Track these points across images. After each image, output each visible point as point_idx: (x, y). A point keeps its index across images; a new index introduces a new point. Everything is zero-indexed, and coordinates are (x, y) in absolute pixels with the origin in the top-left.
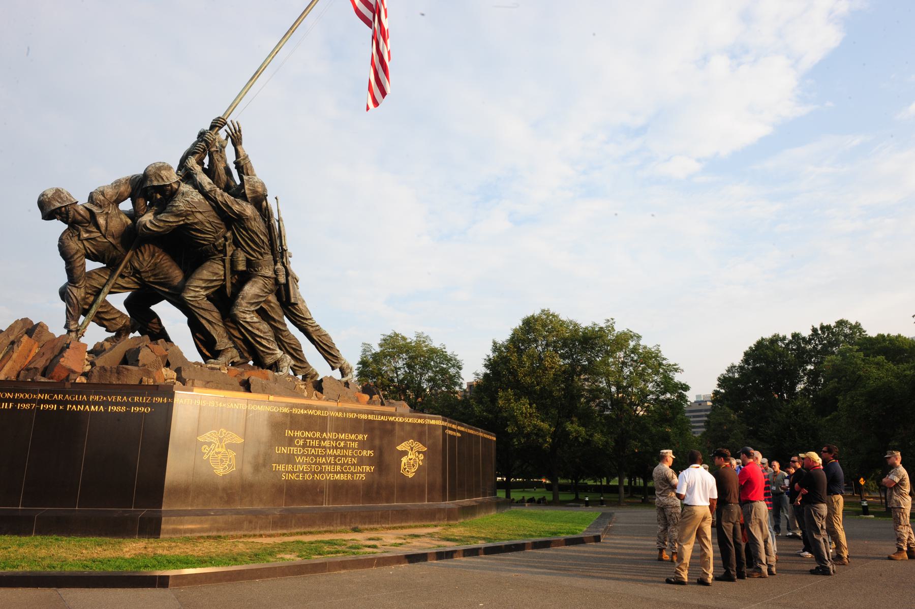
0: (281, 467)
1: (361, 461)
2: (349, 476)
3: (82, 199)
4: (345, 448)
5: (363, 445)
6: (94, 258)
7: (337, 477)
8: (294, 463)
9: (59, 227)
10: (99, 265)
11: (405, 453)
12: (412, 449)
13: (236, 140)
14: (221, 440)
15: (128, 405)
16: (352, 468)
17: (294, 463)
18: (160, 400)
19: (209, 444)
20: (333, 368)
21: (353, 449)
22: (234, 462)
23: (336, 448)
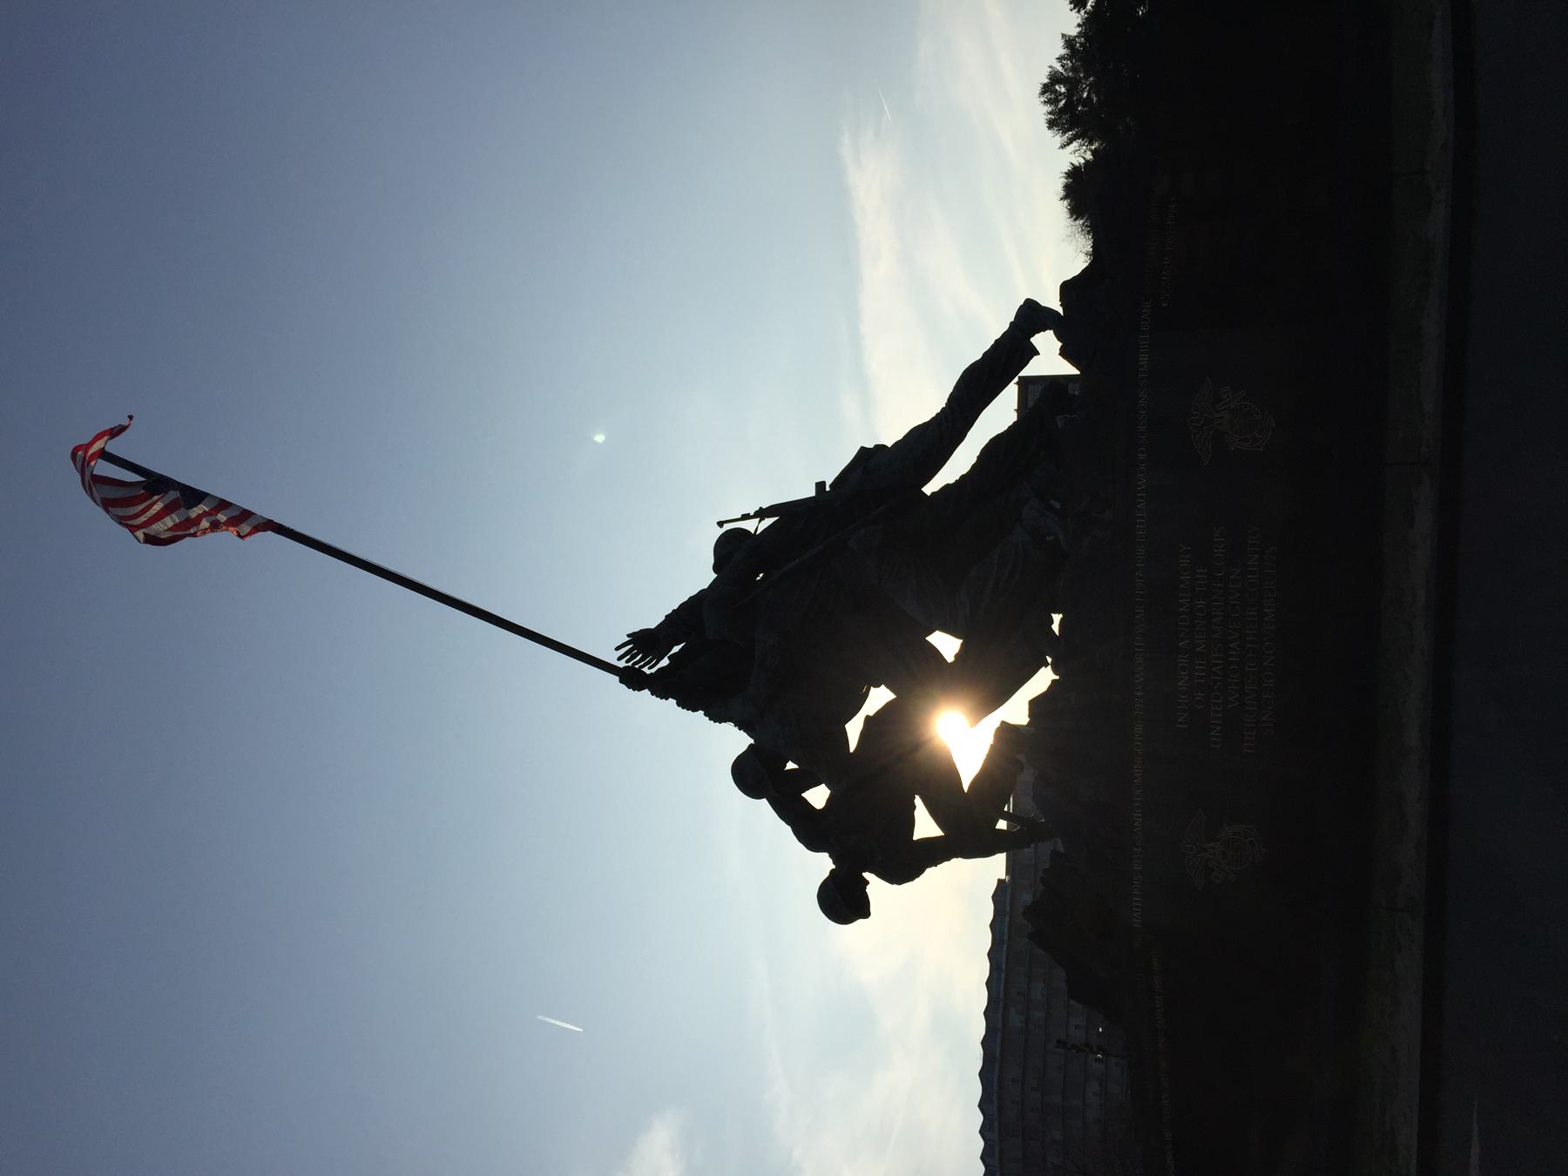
3: (822, 865)
6: (910, 823)
9: (876, 887)
13: (644, 642)
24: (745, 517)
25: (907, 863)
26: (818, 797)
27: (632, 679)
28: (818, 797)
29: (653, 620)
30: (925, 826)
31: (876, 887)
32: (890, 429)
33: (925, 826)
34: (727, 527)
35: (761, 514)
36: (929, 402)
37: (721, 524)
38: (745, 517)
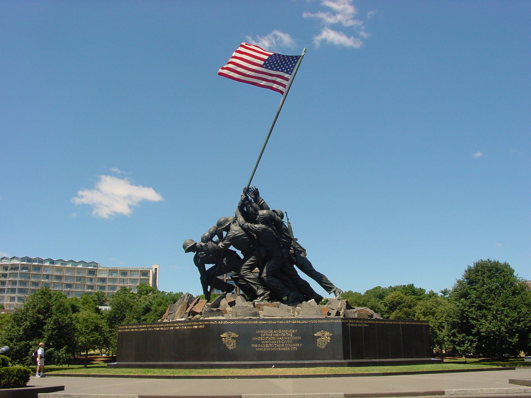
0: (256, 346)
1: (295, 342)
2: (289, 348)
3: (198, 241)
4: (286, 336)
5: (294, 335)
7: (283, 349)
8: (261, 343)
9: (192, 254)
10: (211, 265)
11: (320, 337)
12: (323, 335)
13: (256, 193)
14: (229, 336)
15: (198, 325)
16: (290, 345)
17: (261, 343)
18: (206, 323)
19: (225, 338)
20: (330, 294)
21: (290, 337)
22: (235, 344)
23: (281, 337)
24: (288, 219)
25: (199, 263)
26: (216, 238)
27: (247, 191)
28: (216, 238)
29: (262, 195)
30: (208, 267)
31: (192, 254)
32: (310, 257)
33: (208, 267)
34: (285, 214)
35: (289, 223)
36: (317, 268)
37: (286, 213)
38: (288, 219)
